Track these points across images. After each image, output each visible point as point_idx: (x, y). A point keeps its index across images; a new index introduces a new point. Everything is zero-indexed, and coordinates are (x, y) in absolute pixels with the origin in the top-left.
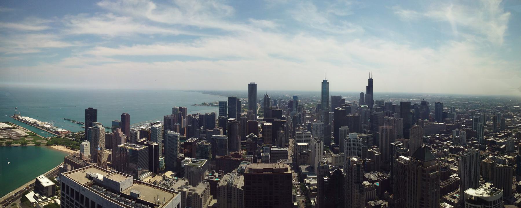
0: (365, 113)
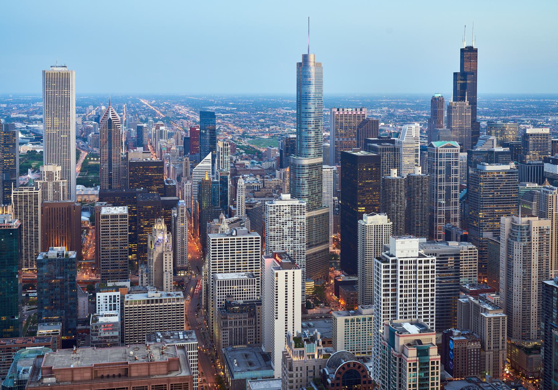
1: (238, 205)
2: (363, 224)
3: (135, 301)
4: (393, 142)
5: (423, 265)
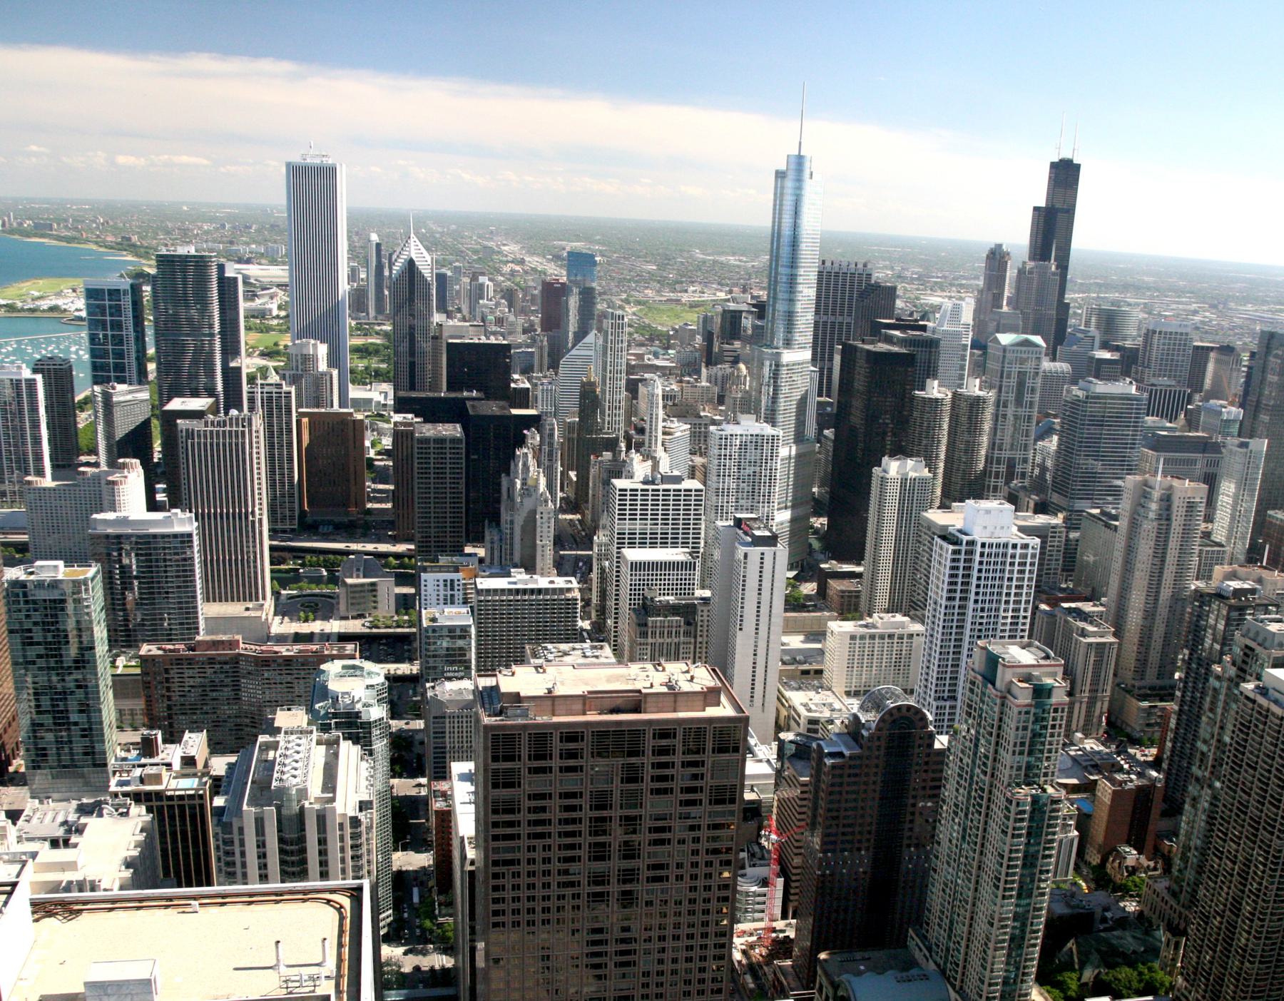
0: (1021, 384)
1: (648, 430)
2: (881, 475)
3: (495, 591)
4: (924, 328)
5: (1019, 551)
